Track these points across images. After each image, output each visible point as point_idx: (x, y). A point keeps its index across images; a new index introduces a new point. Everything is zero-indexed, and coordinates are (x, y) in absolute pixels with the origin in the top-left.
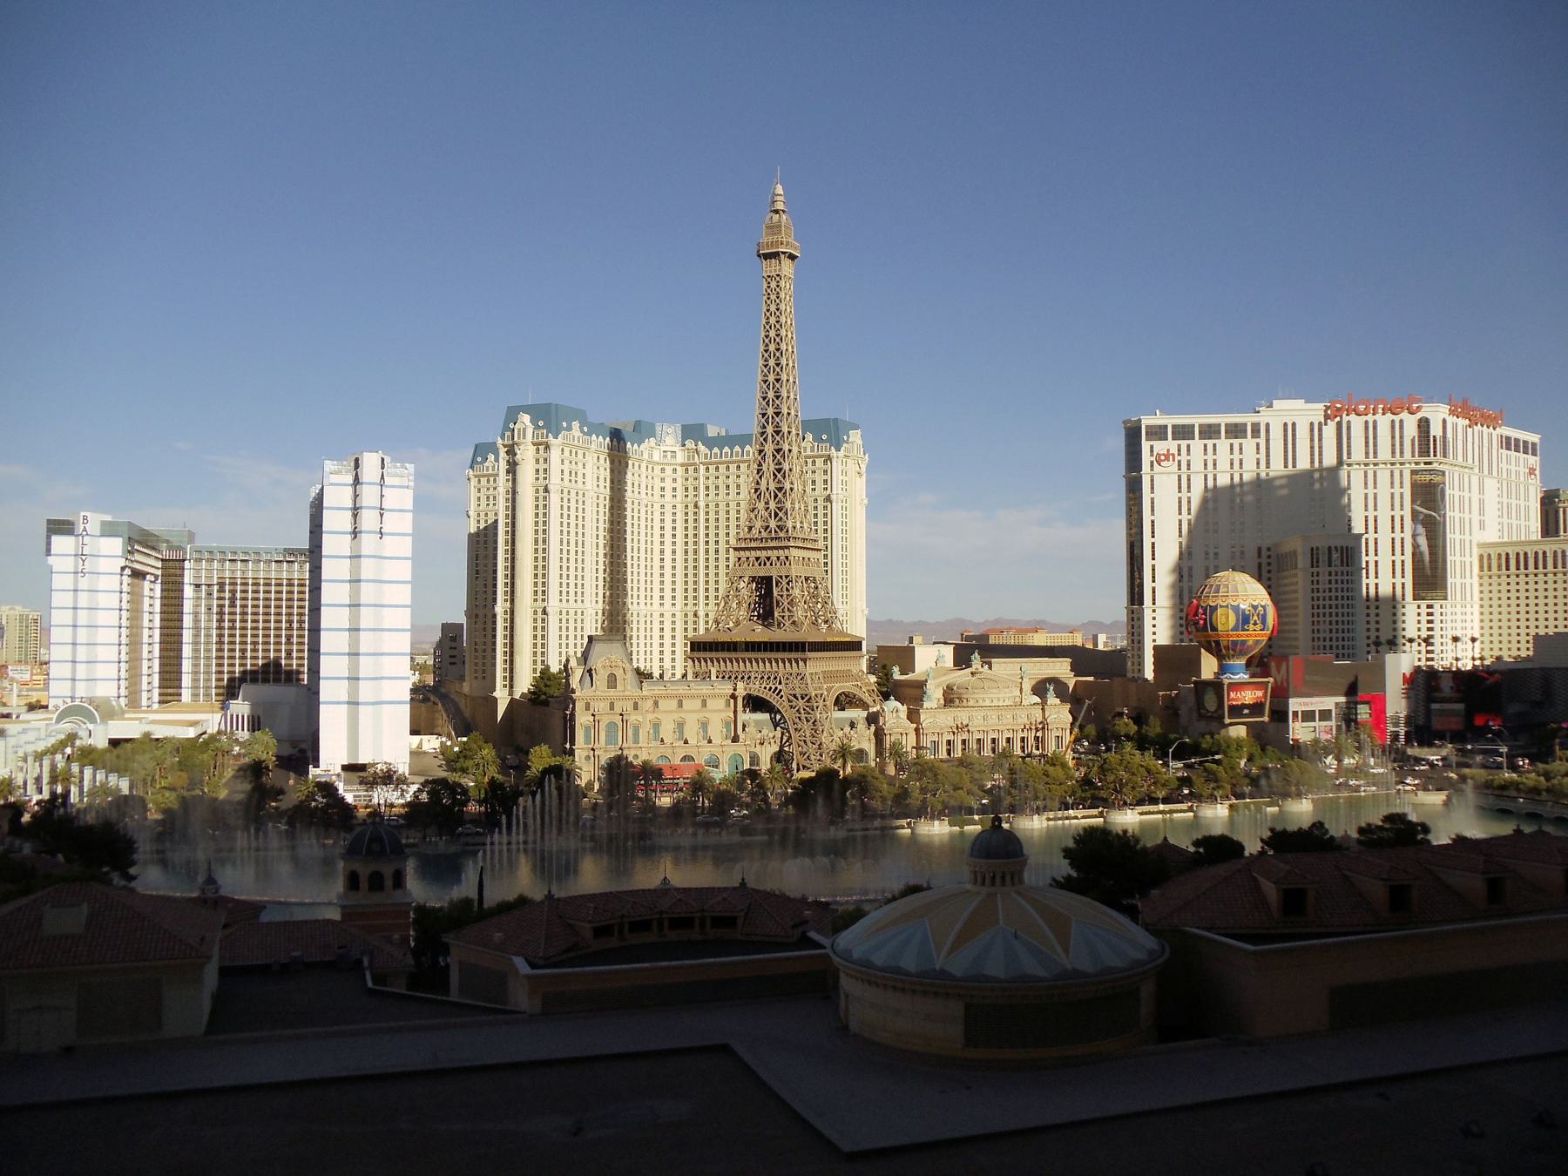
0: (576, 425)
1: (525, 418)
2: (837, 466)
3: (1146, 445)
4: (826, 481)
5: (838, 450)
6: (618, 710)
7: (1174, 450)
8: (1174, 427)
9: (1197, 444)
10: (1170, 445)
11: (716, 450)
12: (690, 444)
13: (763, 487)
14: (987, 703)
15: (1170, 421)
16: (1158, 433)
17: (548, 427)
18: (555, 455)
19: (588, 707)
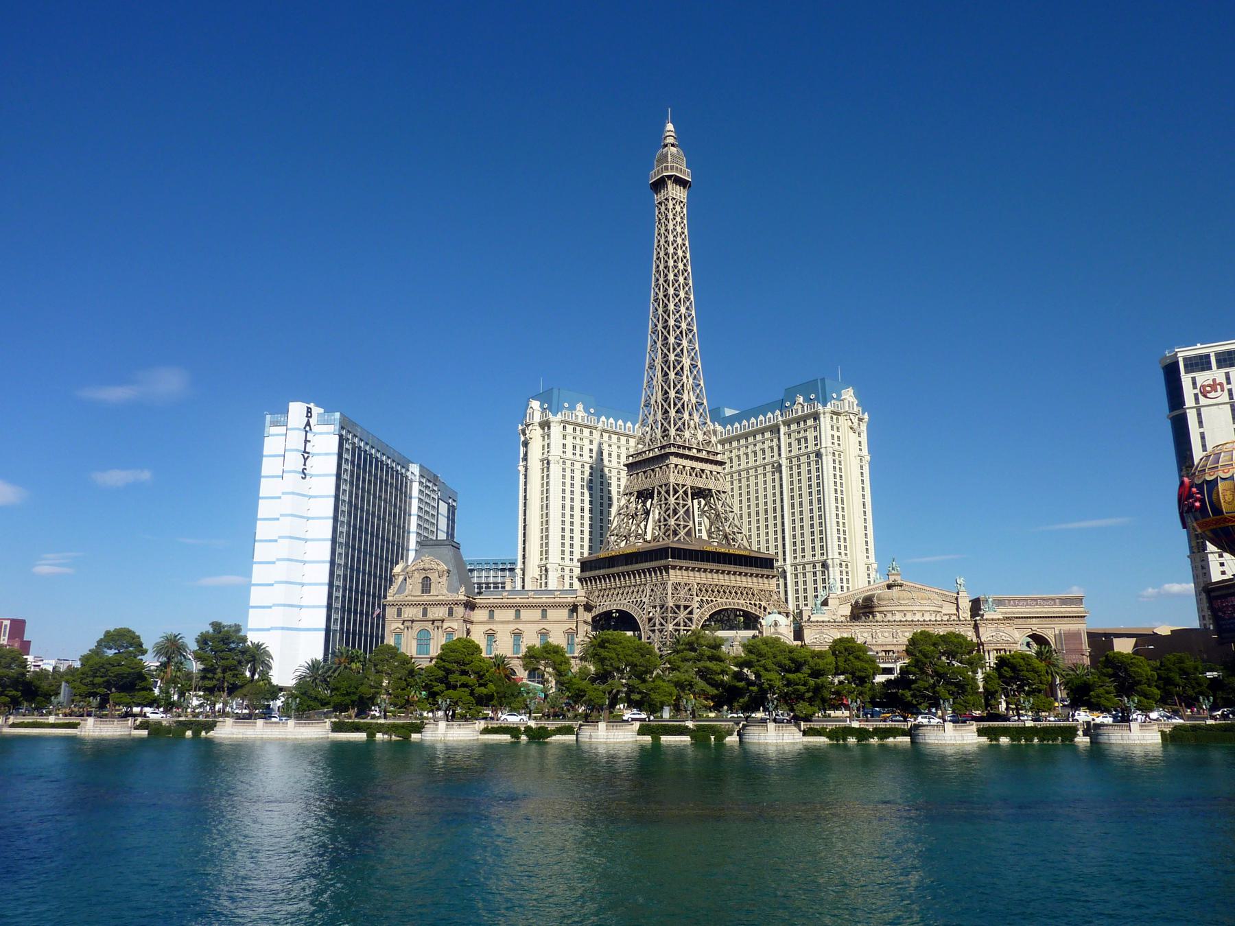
2: (825, 421)
3: (1186, 379)
5: (824, 405)
6: (430, 616)
7: (1221, 378)
8: (1217, 354)
10: (1216, 374)
11: (729, 427)
13: (653, 402)
14: (898, 617)
15: (1212, 349)
16: (1201, 363)
17: (550, 408)
18: (556, 430)
19: (399, 615)
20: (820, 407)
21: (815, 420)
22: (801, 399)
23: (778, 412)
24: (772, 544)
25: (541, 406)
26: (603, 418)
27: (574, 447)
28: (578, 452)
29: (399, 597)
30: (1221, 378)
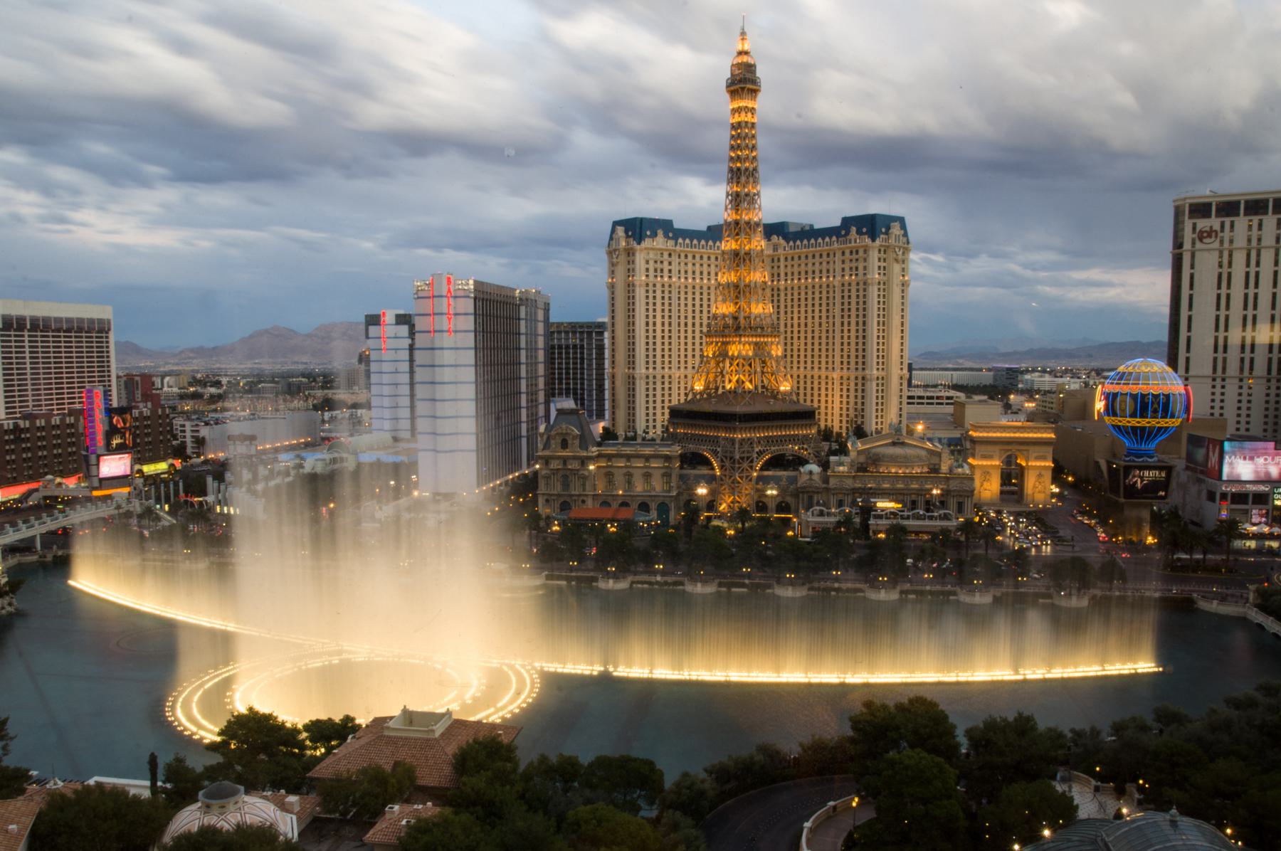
0: (660, 232)
1: (620, 231)
2: (874, 256)
4: (865, 268)
5: (873, 240)
7: (1217, 227)
9: (1241, 222)
10: (1214, 222)
11: (791, 243)
12: (775, 238)
18: (640, 258)
20: (868, 241)
21: (865, 251)
22: (854, 229)
23: (834, 238)
24: (816, 398)
25: (626, 232)
26: (680, 240)
27: (656, 270)
28: (659, 274)
29: (547, 453)
30: (1217, 227)
